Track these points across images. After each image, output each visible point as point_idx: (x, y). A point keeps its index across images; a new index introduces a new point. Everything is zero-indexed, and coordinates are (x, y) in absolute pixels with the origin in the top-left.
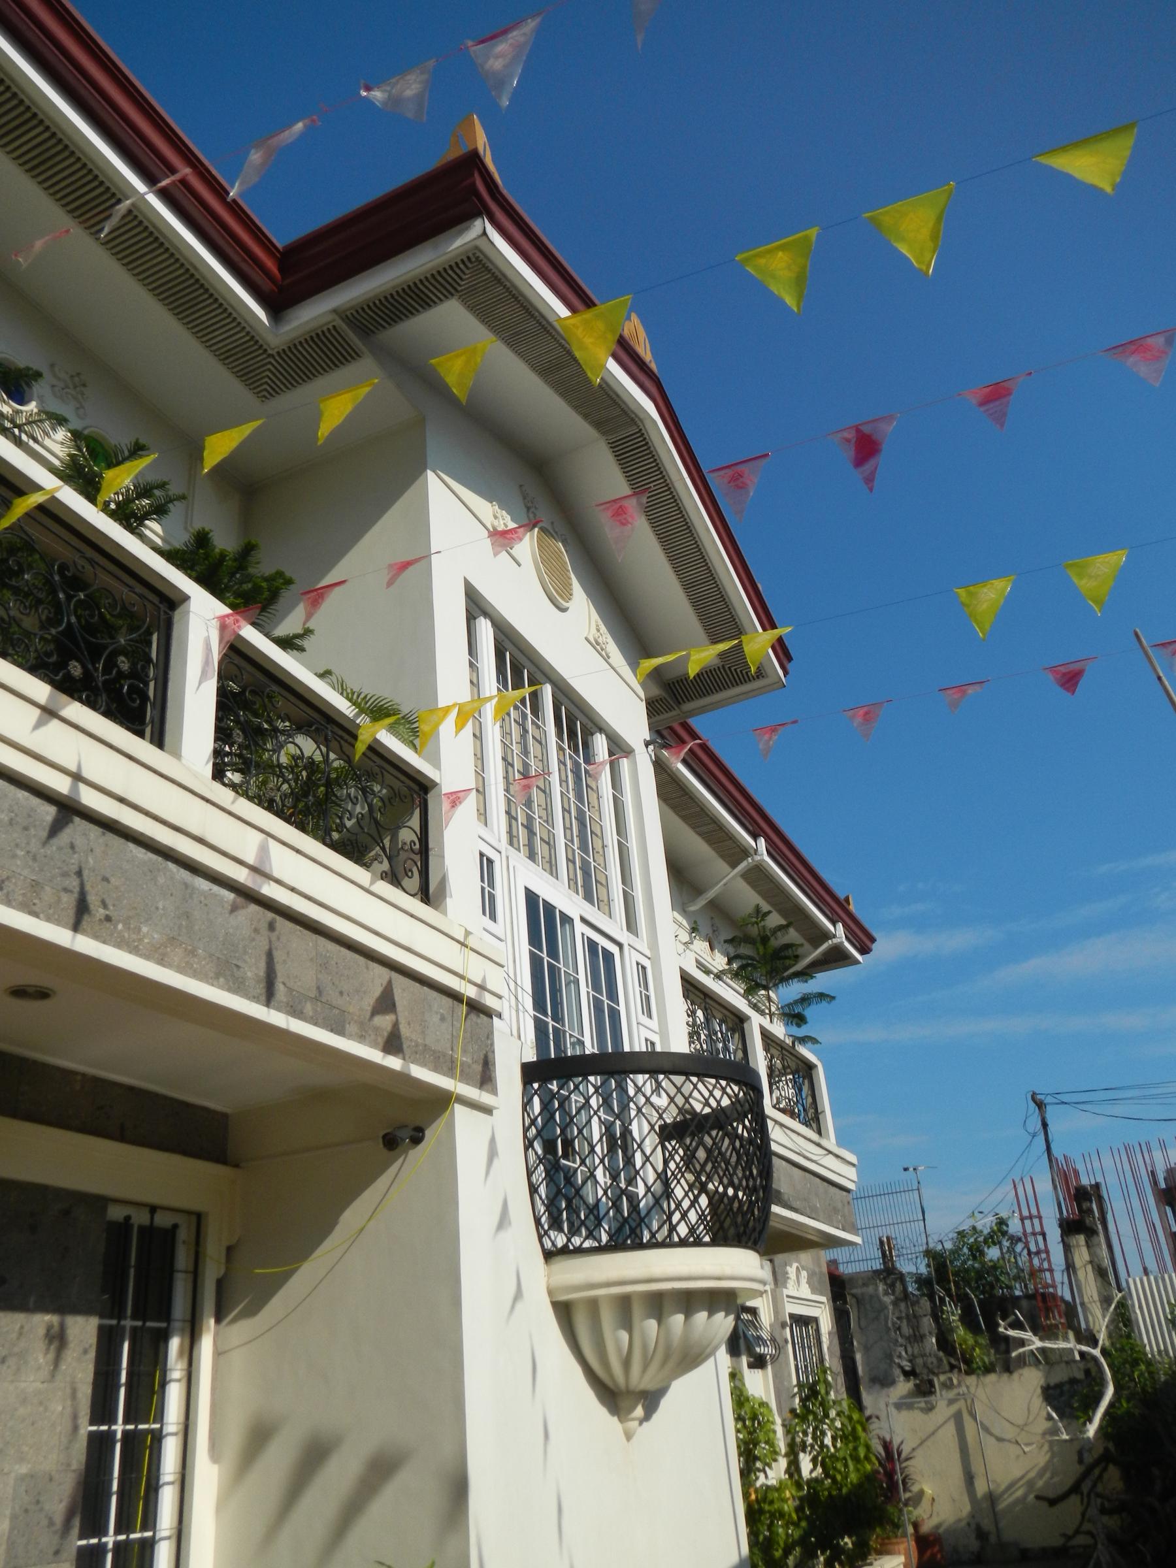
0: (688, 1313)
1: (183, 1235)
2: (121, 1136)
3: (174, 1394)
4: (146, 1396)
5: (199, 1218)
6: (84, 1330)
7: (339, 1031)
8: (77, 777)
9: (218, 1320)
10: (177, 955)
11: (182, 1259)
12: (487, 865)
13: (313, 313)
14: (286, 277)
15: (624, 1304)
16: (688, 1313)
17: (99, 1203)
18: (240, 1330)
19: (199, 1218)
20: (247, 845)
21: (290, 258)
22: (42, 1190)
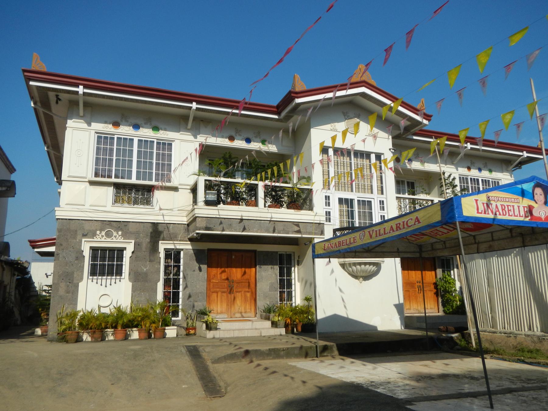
0: (365, 266)
1: (293, 255)
2: (279, 244)
3: (293, 274)
4: (289, 274)
5: (294, 252)
6: (277, 268)
7: (288, 234)
8: (242, 216)
9: (298, 265)
10: (259, 231)
11: (293, 258)
12: (327, 198)
13: (283, 114)
14: (278, 110)
15: (350, 264)
16: (365, 266)
17: (277, 252)
18: (300, 267)
19: (294, 252)
20: (269, 215)
21: (278, 107)
22: (268, 252)
